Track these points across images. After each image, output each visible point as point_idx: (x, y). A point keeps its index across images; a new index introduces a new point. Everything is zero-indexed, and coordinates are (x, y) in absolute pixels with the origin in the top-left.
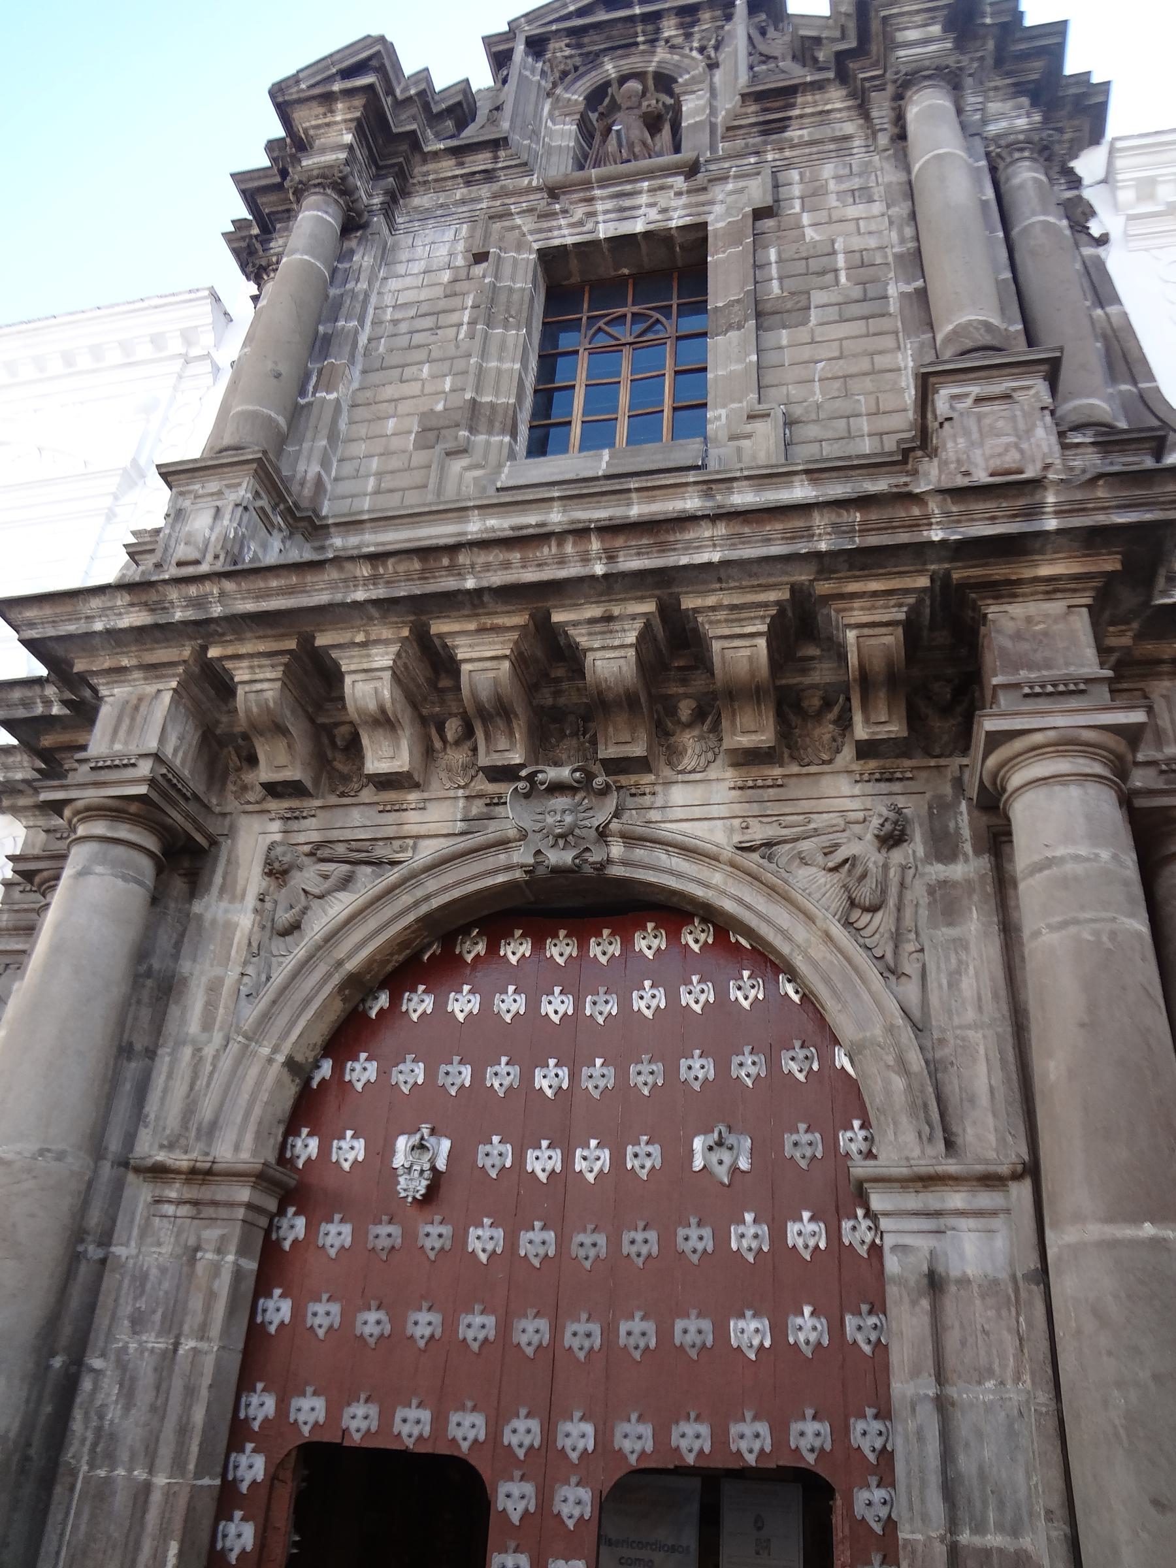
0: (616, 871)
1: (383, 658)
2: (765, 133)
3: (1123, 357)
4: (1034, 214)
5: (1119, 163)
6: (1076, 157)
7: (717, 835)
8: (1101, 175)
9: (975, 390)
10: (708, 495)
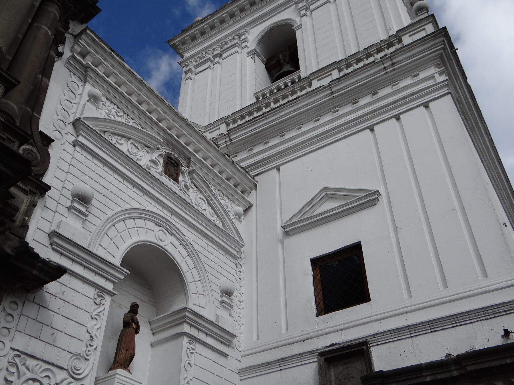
3: (36, 98)
4: (46, 25)
5: (83, 36)
6: (73, 20)
8: (76, 33)
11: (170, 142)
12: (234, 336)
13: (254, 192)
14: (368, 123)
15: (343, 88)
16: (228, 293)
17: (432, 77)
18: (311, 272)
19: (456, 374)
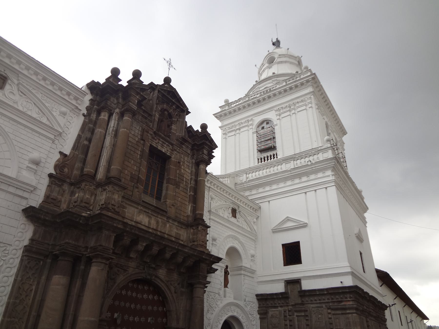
0: (153, 280)
1: (144, 244)
2: (181, 143)
7: (162, 277)
9: (203, 228)
10: (167, 219)
11: (234, 203)
12: (256, 271)
13: (259, 210)
14: (304, 190)
15: (295, 172)
16: (253, 256)
17: (329, 176)
18: (282, 249)
19: (326, 293)
